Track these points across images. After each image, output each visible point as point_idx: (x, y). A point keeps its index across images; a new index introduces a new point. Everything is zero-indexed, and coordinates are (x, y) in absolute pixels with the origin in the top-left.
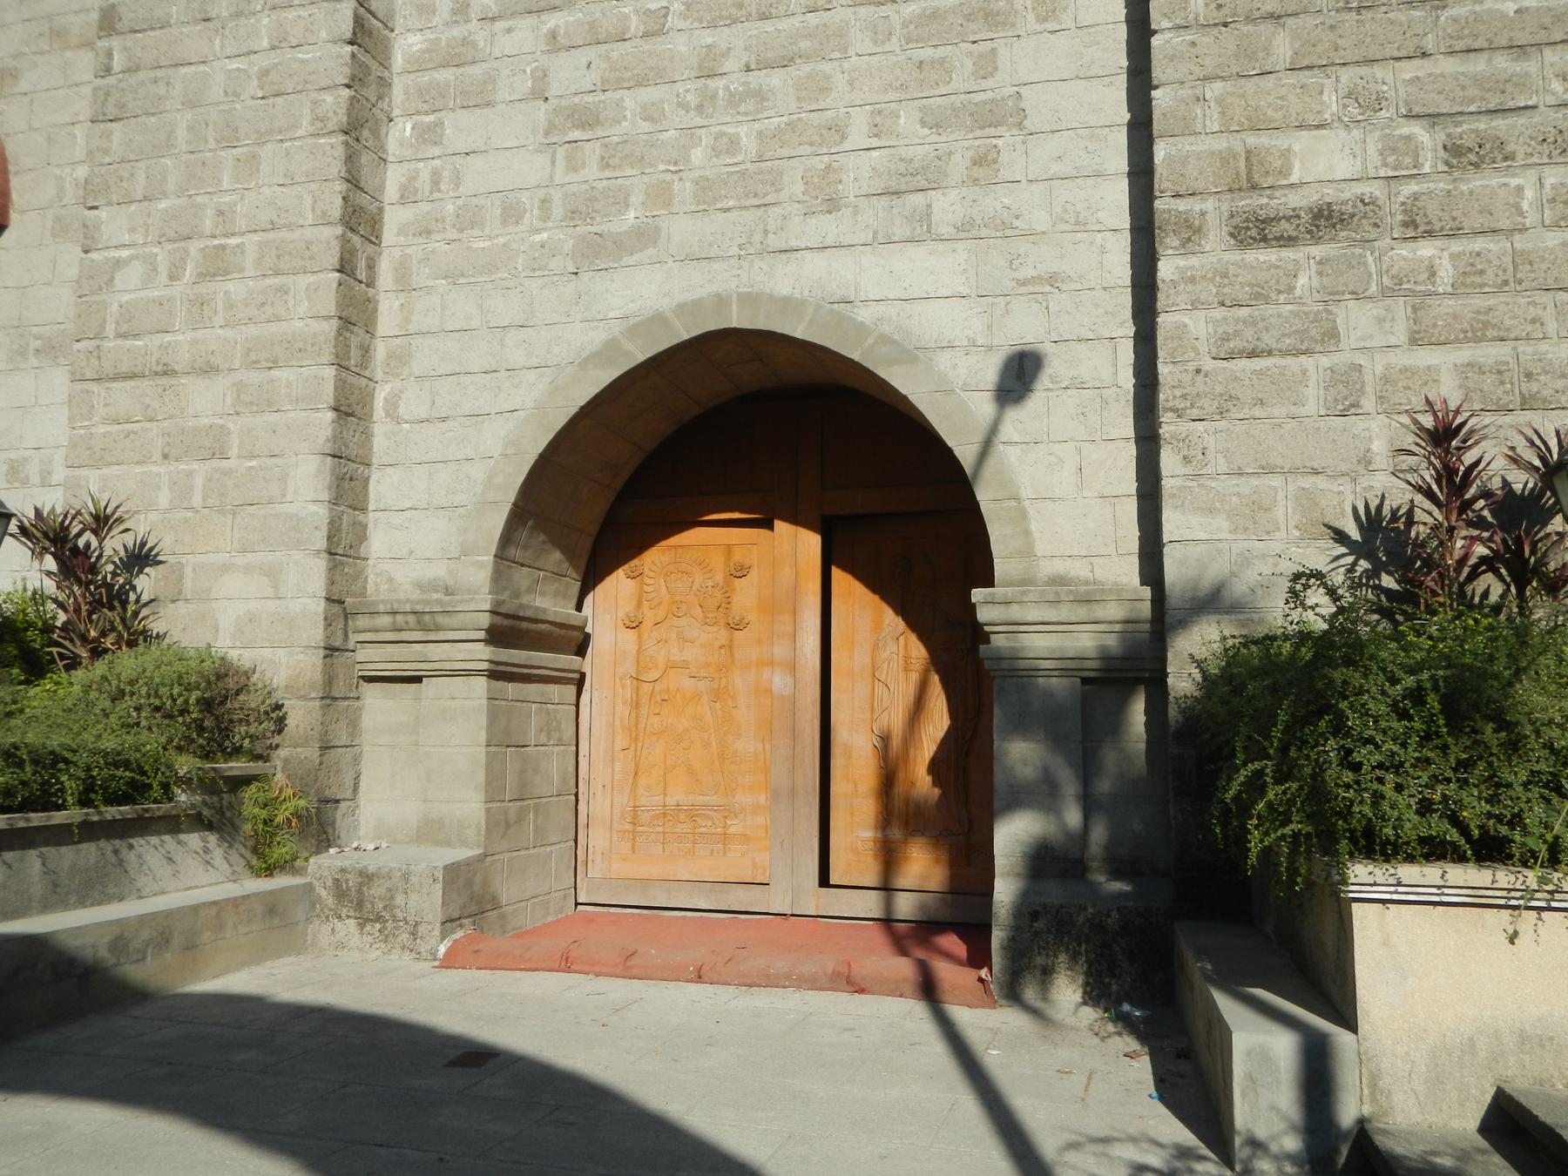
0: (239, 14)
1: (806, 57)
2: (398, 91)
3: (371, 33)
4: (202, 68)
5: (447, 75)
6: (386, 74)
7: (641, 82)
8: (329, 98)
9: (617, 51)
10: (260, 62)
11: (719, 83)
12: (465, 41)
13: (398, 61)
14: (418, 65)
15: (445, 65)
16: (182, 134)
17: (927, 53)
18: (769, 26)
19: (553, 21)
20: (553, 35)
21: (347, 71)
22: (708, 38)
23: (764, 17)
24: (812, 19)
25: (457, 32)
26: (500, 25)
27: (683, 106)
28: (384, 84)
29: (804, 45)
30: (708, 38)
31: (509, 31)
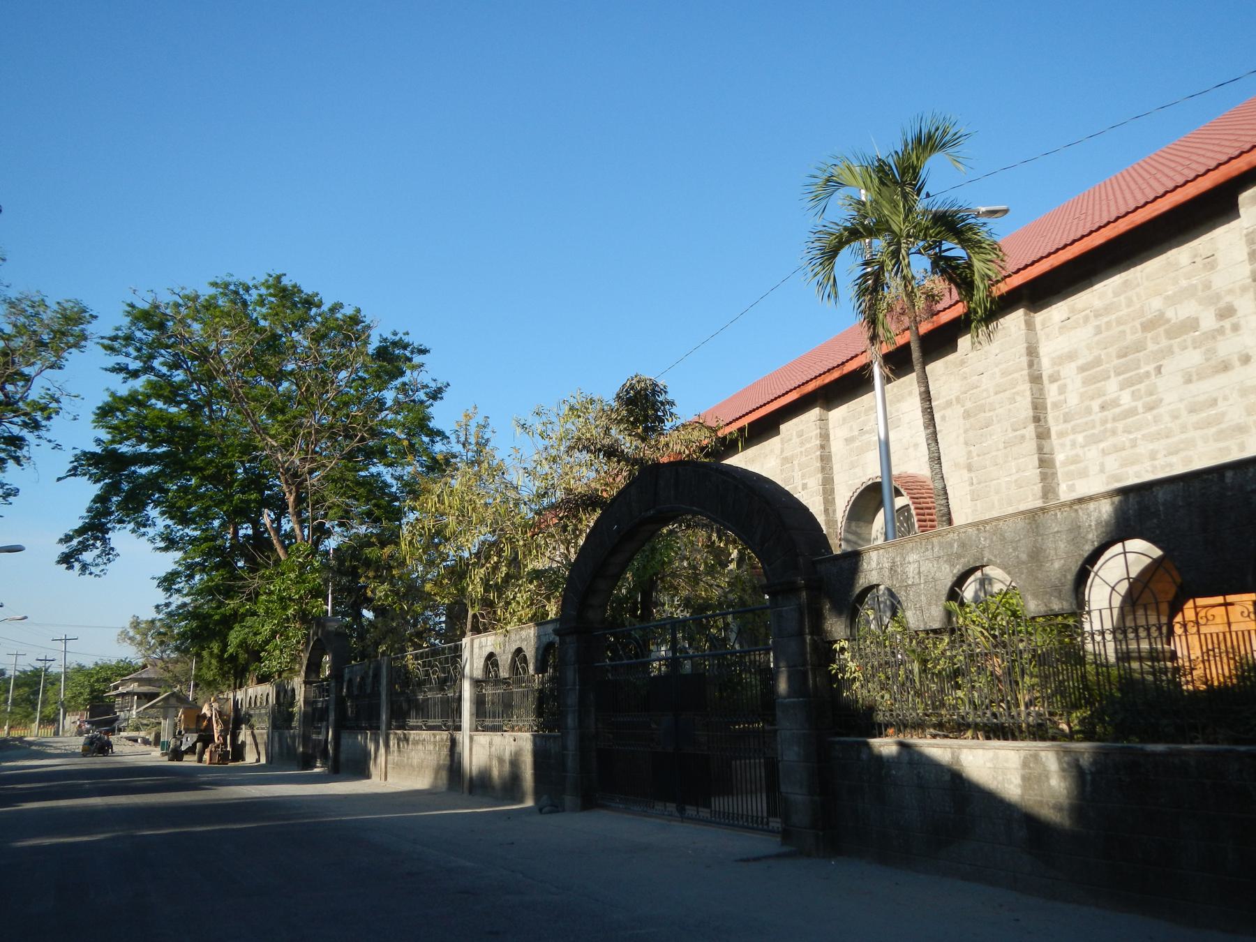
0: (1005, 462)
1: (1182, 450)
2: (1059, 475)
3: (1045, 461)
4: (999, 481)
5: (1072, 467)
6: (1054, 470)
7: (1133, 463)
8: (1036, 488)
9: (1124, 453)
10: (1014, 477)
11: (1156, 463)
12: (1077, 455)
13: (1058, 464)
14: (1064, 464)
15: (1072, 464)
16: (996, 503)
17: (1222, 445)
18: (1170, 441)
19: (1102, 445)
20: (1103, 450)
21: (1039, 478)
22: (1151, 446)
23: (1167, 437)
24: (1183, 436)
25: (1073, 452)
26: (1086, 449)
27: (1147, 471)
28: (1054, 474)
29: (1182, 446)
30: (1151, 446)
31: (1089, 450)
